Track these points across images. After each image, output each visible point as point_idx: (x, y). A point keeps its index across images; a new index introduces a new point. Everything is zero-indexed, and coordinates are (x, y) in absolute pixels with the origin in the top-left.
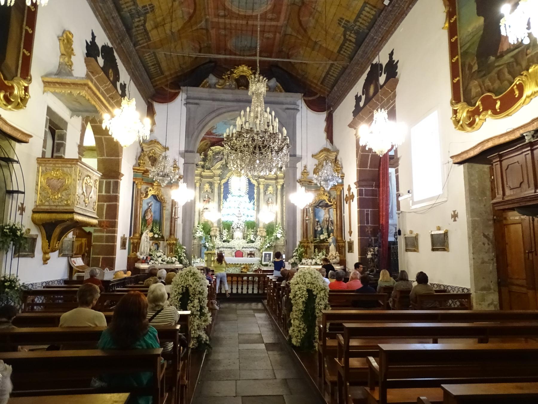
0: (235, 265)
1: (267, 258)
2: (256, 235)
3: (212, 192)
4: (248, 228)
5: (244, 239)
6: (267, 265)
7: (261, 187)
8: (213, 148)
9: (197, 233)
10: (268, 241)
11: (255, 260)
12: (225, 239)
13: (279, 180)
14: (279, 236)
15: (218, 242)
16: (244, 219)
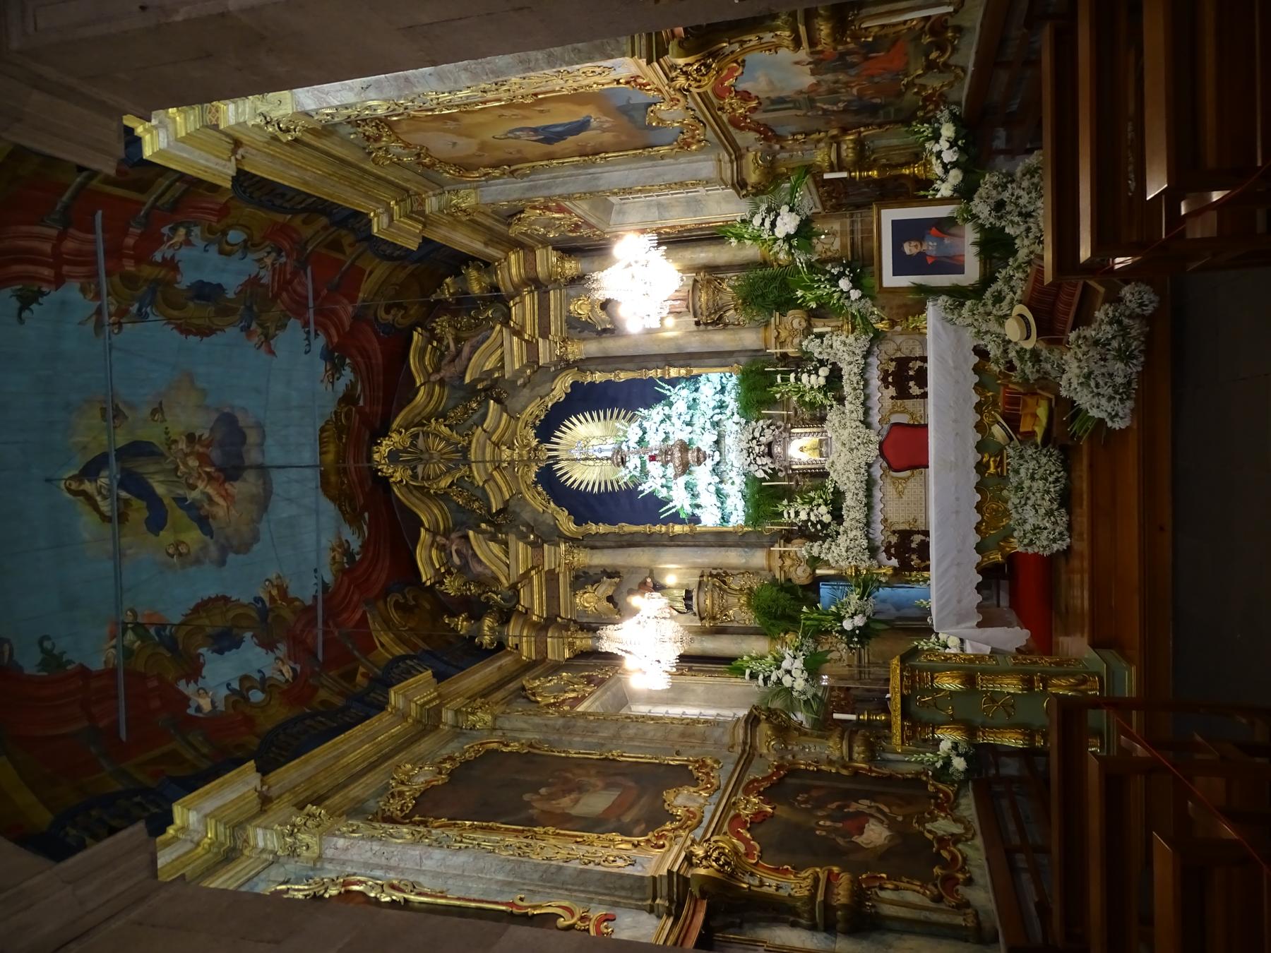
0: (990, 484)
1: (930, 247)
2: (801, 362)
3: (610, 576)
4: (772, 403)
5: (823, 420)
6: (996, 247)
7: (576, 350)
8: (426, 576)
9: (787, 681)
10: (825, 289)
11: (941, 340)
12: (823, 513)
13: (541, 271)
14: (787, 223)
15: (841, 553)
16: (732, 425)
